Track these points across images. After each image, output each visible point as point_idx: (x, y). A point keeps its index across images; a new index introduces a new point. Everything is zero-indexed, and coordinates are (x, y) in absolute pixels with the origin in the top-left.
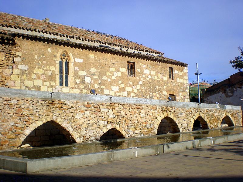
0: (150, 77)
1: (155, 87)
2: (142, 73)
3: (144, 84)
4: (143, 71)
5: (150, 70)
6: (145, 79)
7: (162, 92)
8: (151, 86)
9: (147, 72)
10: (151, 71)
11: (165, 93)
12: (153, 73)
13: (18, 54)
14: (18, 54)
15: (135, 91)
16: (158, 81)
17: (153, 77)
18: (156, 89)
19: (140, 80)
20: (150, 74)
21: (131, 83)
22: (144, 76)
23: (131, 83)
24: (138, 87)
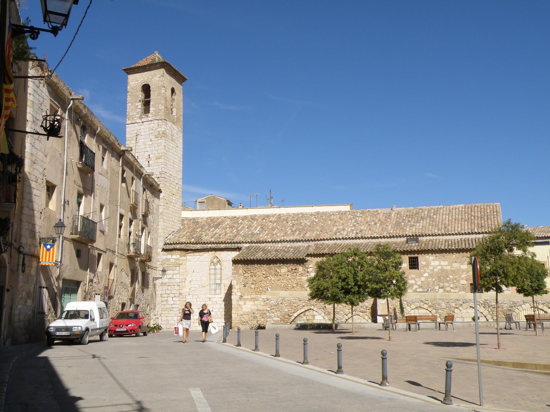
0: (440, 268)
1: (447, 277)
2: (428, 265)
3: (431, 275)
4: (430, 263)
5: (440, 261)
6: (433, 270)
7: (458, 281)
8: (442, 277)
9: (437, 263)
10: (442, 262)
11: (464, 282)
12: (443, 263)
13: (310, 266)
14: (310, 266)
15: (419, 283)
16: (452, 271)
17: (444, 268)
18: (448, 279)
19: (425, 272)
20: (440, 265)
21: (413, 276)
22: (431, 268)
23: (413, 276)
24: (423, 279)
